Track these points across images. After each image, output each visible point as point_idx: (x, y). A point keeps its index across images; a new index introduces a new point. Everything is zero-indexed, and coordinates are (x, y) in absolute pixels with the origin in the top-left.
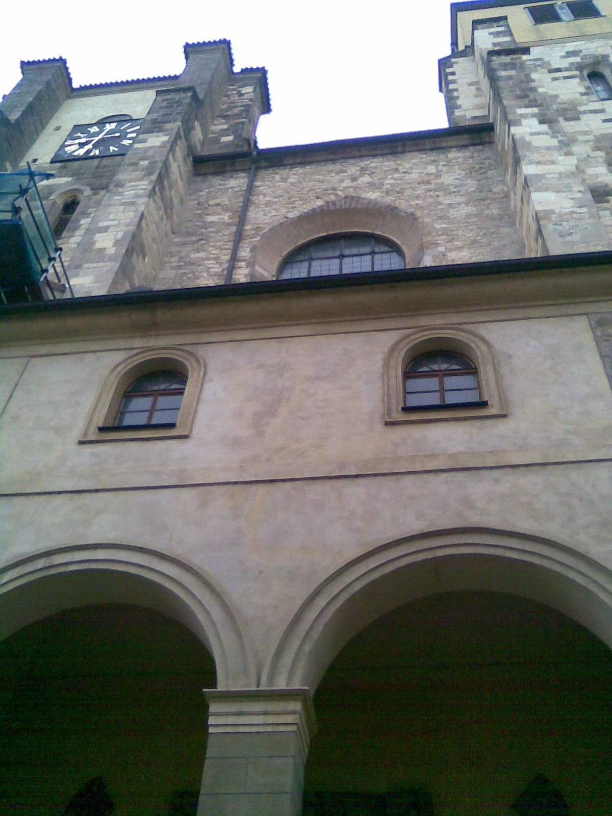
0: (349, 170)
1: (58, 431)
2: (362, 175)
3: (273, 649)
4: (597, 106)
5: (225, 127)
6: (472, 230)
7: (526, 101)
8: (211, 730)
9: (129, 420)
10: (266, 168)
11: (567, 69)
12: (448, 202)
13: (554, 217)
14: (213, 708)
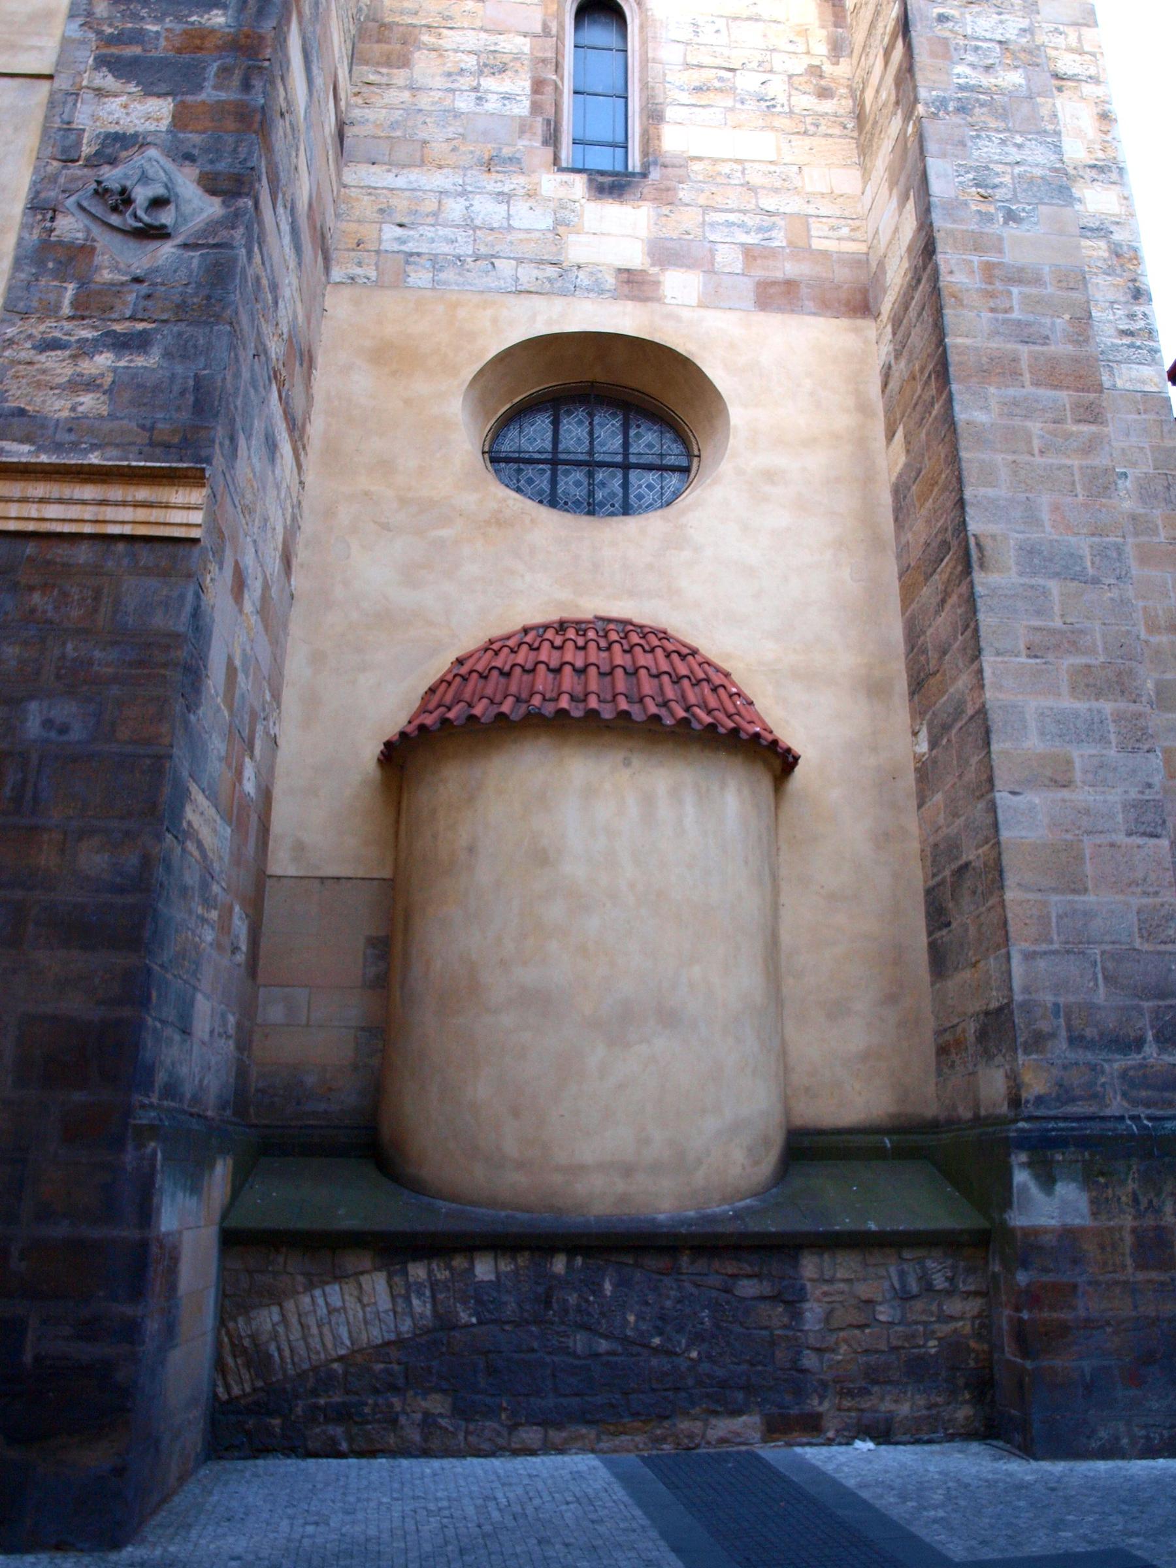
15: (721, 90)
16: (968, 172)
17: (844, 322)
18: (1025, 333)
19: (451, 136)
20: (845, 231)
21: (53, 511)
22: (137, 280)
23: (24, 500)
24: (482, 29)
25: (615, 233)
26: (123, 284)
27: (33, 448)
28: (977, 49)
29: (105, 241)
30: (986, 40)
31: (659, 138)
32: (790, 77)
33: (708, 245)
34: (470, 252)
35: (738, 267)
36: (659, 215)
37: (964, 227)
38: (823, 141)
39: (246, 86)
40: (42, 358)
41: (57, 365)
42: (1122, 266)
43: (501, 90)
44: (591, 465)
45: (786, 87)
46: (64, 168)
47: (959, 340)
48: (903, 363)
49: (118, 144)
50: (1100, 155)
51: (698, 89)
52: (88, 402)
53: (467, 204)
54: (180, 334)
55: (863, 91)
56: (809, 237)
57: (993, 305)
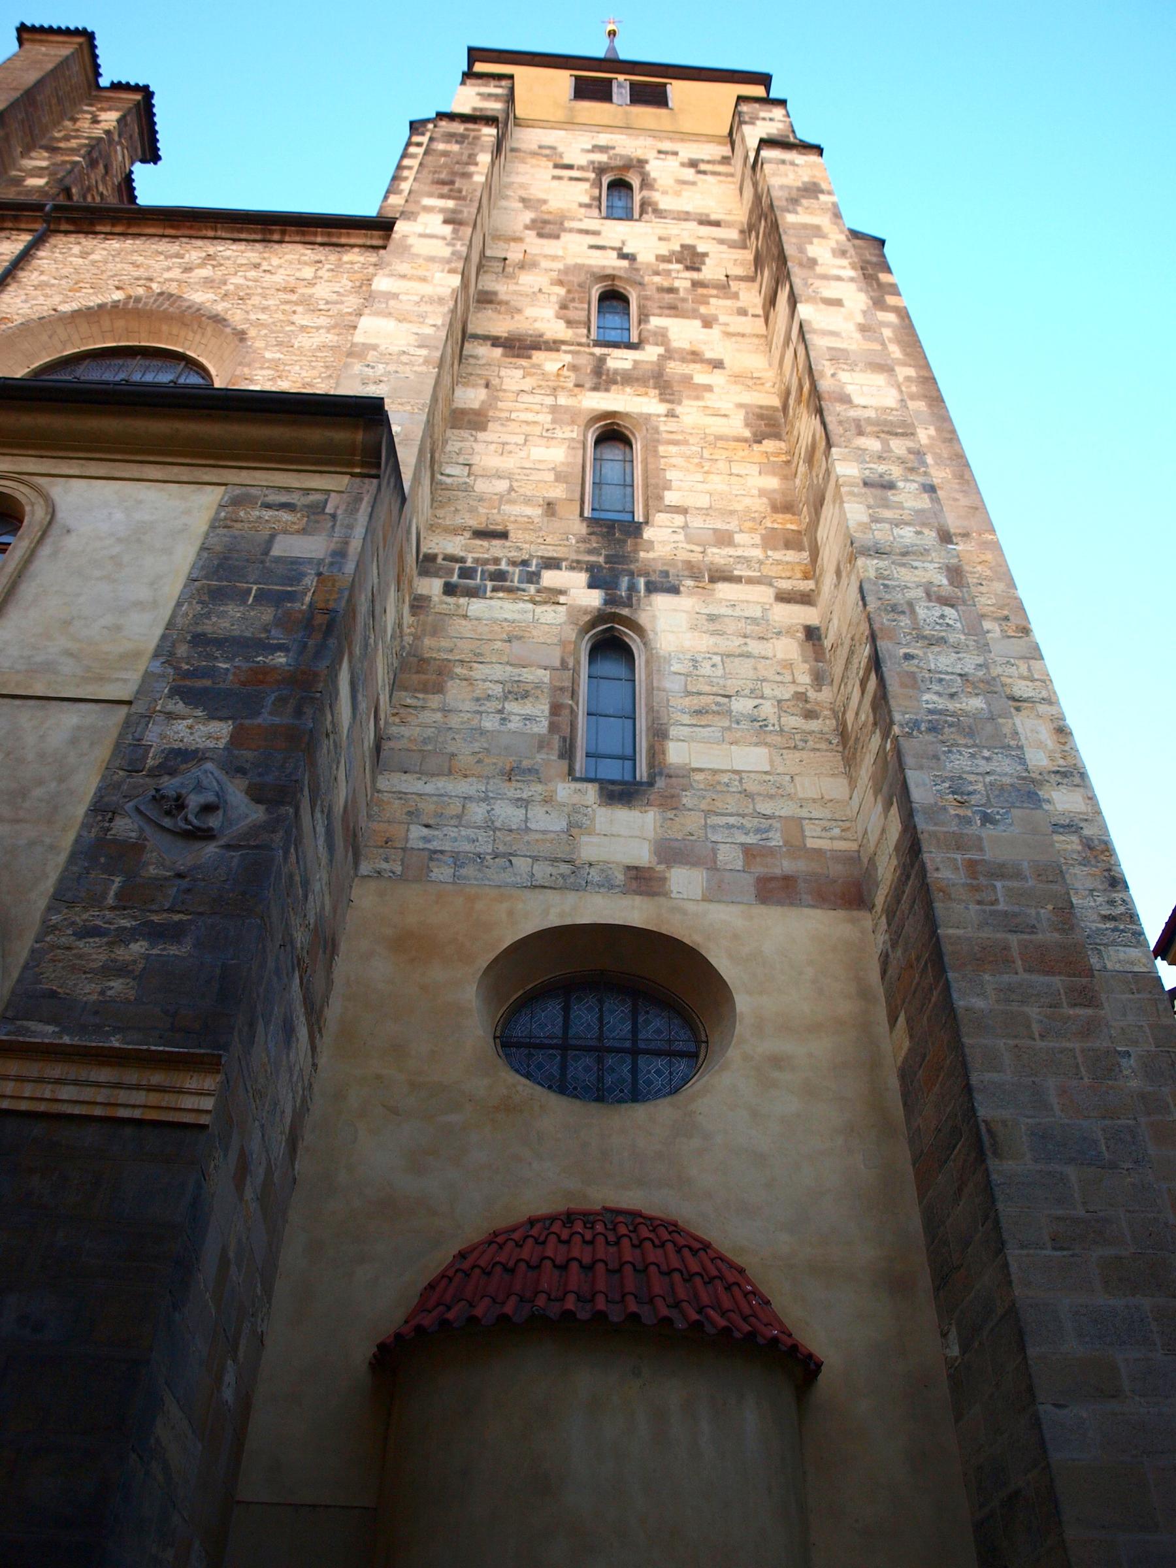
0: (187, 256)
2: (202, 265)
4: (593, 224)
5: (44, 164)
6: (314, 368)
7: (445, 189)
10: (67, 233)
11: (581, 168)
12: (305, 323)
13: (371, 356)
15: (718, 713)
16: (943, 782)
17: (841, 914)
18: (1012, 923)
19: (477, 750)
20: (837, 831)
21: (66, 1092)
22: (180, 876)
23: (40, 1080)
24: (507, 663)
25: (625, 835)
26: (166, 879)
27: (57, 1029)
28: (941, 680)
29: (155, 839)
30: (947, 673)
31: (664, 753)
32: (779, 702)
33: (710, 845)
34: (490, 851)
35: (739, 864)
36: (665, 819)
37: (945, 829)
38: (812, 754)
39: (299, 713)
40: (81, 944)
41: (92, 951)
42: (1095, 857)
43: (522, 712)
44: (599, 1050)
45: (776, 710)
46: (128, 777)
47: (951, 931)
48: (899, 953)
49: (180, 758)
50: (1061, 762)
51: (698, 712)
52: (117, 986)
53: (489, 808)
55: (844, 713)
56: (804, 837)
57: (979, 898)
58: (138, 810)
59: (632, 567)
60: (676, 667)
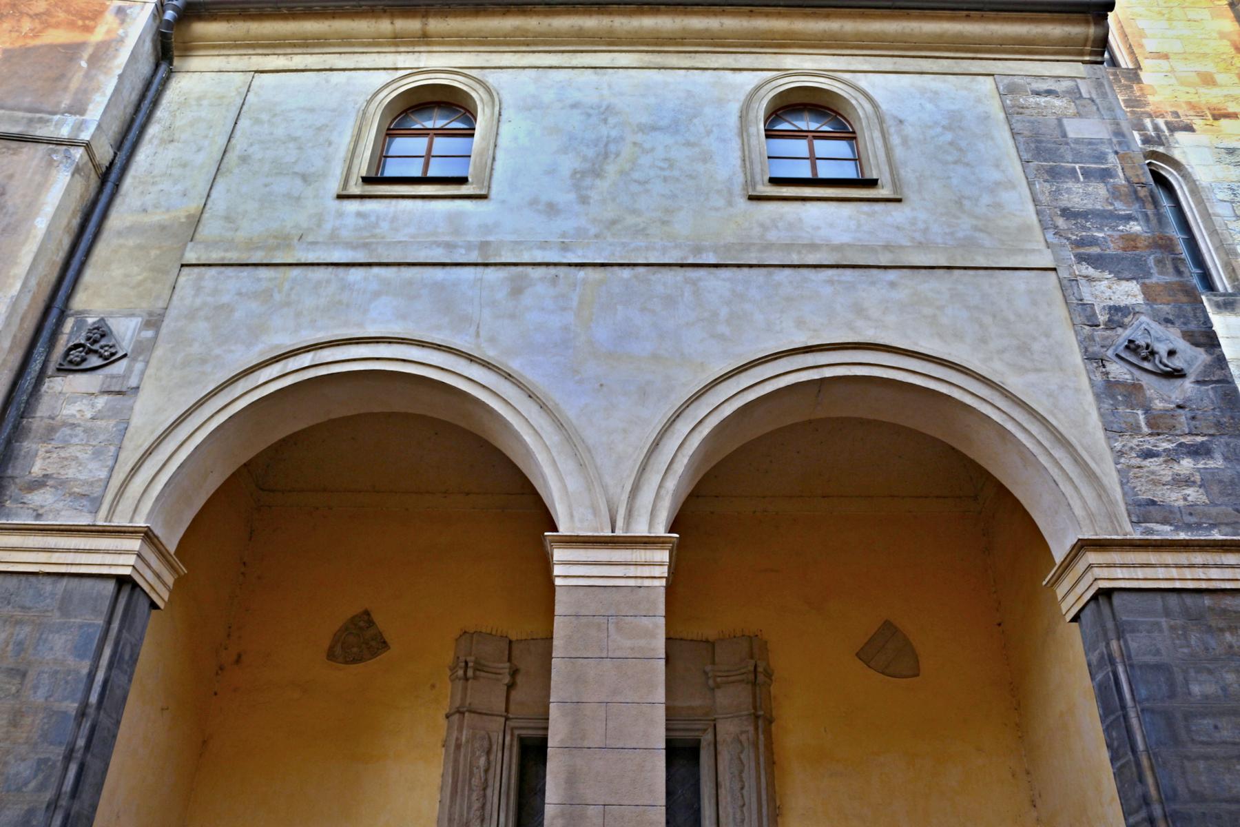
1: (305, 178)
3: (628, 488)
8: (558, 582)
9: (392, 170)
14: (559, 554)
21: (1214, 573)
22: (1179, 407)
52: (1193, 494)
54: (1227, 445)
58: (1118, 356)
59: (1148, 109)
60: (1220, 196)
